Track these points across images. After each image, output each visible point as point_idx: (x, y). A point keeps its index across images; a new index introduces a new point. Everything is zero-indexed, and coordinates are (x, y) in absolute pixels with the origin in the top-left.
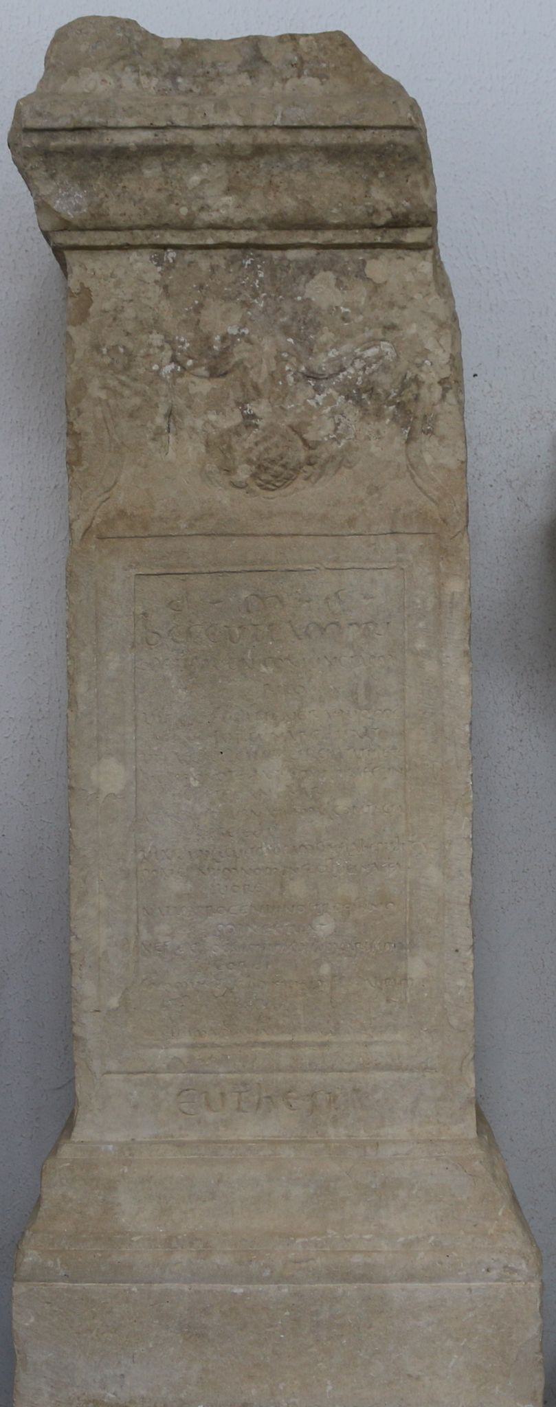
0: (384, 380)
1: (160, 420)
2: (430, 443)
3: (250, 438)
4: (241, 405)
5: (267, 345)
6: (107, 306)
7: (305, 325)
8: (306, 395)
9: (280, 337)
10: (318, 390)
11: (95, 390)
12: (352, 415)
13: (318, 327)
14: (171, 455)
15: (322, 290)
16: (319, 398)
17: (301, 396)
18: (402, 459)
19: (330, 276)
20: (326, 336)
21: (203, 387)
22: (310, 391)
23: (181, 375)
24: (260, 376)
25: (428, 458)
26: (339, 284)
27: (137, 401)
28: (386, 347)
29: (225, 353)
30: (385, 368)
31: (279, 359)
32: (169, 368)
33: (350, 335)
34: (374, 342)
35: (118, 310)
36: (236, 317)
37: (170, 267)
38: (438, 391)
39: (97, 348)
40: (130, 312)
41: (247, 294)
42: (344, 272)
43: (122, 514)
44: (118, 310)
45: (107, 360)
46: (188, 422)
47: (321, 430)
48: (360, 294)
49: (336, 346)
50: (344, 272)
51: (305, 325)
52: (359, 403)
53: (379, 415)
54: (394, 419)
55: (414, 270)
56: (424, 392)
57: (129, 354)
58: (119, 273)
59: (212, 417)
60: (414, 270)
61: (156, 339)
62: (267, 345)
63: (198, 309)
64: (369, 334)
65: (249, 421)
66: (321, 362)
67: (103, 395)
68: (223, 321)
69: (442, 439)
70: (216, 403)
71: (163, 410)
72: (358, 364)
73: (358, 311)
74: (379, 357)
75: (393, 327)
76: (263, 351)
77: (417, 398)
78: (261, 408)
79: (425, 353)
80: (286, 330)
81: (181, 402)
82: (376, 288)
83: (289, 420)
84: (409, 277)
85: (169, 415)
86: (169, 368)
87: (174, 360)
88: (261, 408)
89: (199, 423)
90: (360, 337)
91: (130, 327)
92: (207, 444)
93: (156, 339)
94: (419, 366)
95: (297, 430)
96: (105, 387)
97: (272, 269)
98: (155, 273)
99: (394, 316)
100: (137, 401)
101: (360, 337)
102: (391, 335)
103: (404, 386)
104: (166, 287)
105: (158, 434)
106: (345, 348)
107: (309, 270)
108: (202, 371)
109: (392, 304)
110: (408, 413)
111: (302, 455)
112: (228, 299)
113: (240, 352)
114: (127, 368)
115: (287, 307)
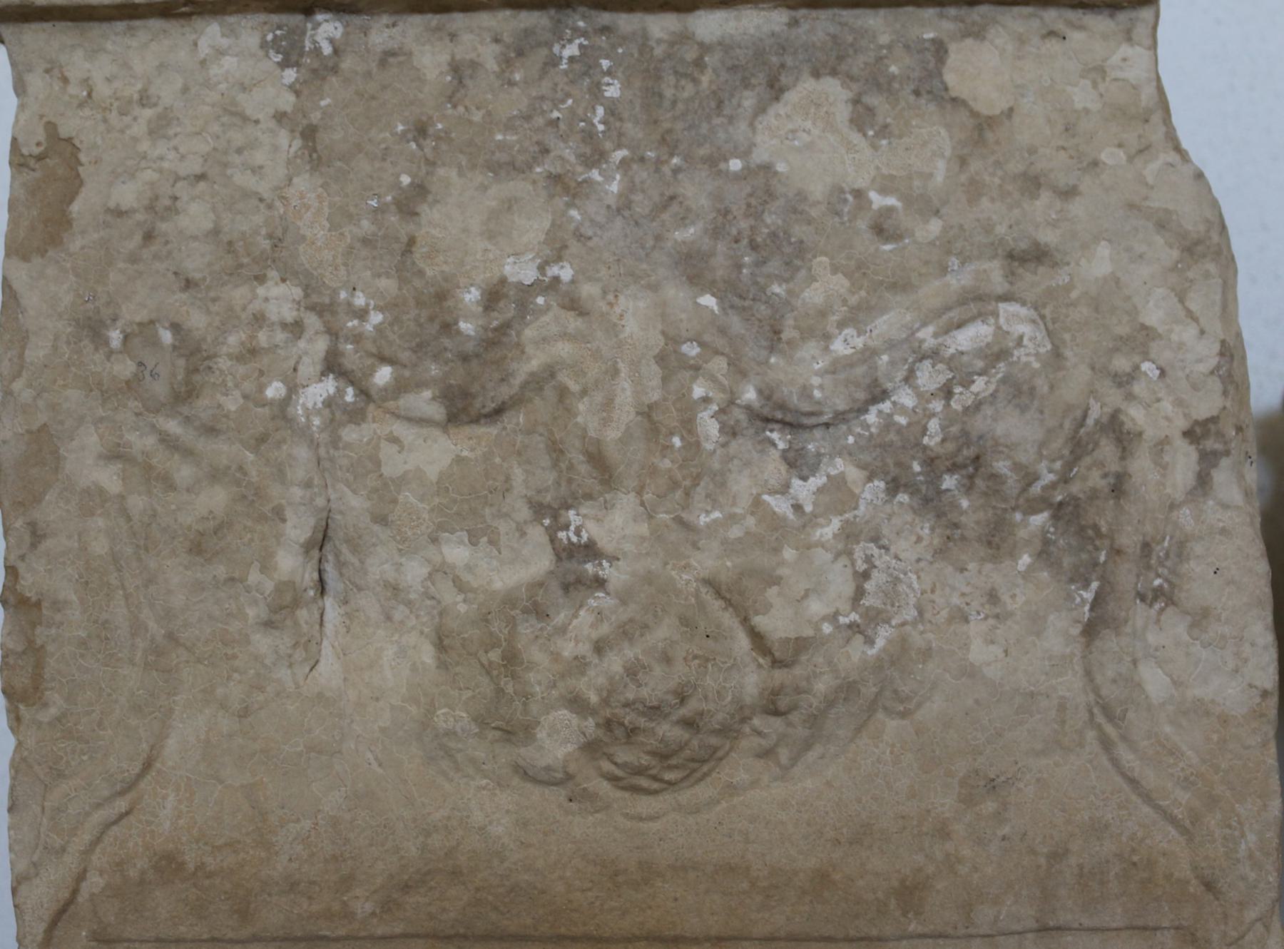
0: (1016, 430)
1: (290, 563)
2: (1163, 633)
3: (582, 623)
4: (549, 512)
5: (634, 317)
6: (127, 194)
7: (754, 252)
8: (759, 478)
9: (676, 293)
10: (797, 463)
11: (87, 464)
12: (909, 540)
13: (797, 258)
14: (329, 667)
15: (808, 140)
16: (804, 490)
17: (742, 485)
18: (1071, 685)
19: (834, 90)
20: (823, 287)
21: (427, 453)
22: (773, 467)
23: (356, 415)
24: (610, 419)
25: (1154, 681)
26: (862, 117)
27: (216, 499)
28: (1016, 320)
29: (497, 340)
30: (1019, 392)
31: (669, 361)
32: (319, 391)
33: (900, 285)
34: (977, 303)
35: (160, 208)
36: (533, 228)
37: (324, 70)
38: (1184, 461)
39: (92, 328)
40: (196, 215)
41: (567, 152)
42: (877, 80)
43: (168, 865)
44: (160, 208)
45: (124, 368)
46: (379, 565)
47: (808, 600)
48: (930, 148)
49: (856, 317)
50: (877, 80)
51: (754, 252)
52: (931, 502)
53: (996, 540)
54: (1045, 553)
55: (1098, 72)
56: (1141, 465)
57: (194, 354)
58: (167, 92)
59: (456, 553)
60: (1098, 72)
61: (279, 298)
62: (634, 317)
63: (410, 202)
64: (960, 279)
65: (577, 566)
66: (809, 372)
67: (108, 478)
68: (487, 238)
69: (1200, 618)
70: (466, 506)
71: (298, 528)
72: (929, 377)
73: (926, 207)
74: (996, 354)
75: (1038, 256)
76: (623, 335)
77: (1119, 487)
78: (614, 524)
79: (1143, 339)
80: (693, 268)
81: (354, 504)
82: (982, 128)
83: (707, 561)
84: (1082, 96)
85: (321, 541)
86: (319, 391)
87: (332, 365)
88: (614, 524)
89: (414, 572)
90: (932, 292)
91: (196, 261)
92: (441, 645)
93: (279, 298)
94: (1124, 381)
95: (733, 595)
96: (116, 454)
97: (648, 71)
98: (276, 89)
99: (1040, 219)
100: (216, 499)
101: (932, 292)
102: (1036, 280)
103: (1079, 448)
104: (309, 134)
105: (283, 606)
106: (886, 325)
107: (769, 75)
108: (424, 402)
109: (1032, 183)
110: (1088, 535)
111: (752, 680)
112: (514, 168)
113: (544, 342)
114: (184, 395)
115: (696, 191)
